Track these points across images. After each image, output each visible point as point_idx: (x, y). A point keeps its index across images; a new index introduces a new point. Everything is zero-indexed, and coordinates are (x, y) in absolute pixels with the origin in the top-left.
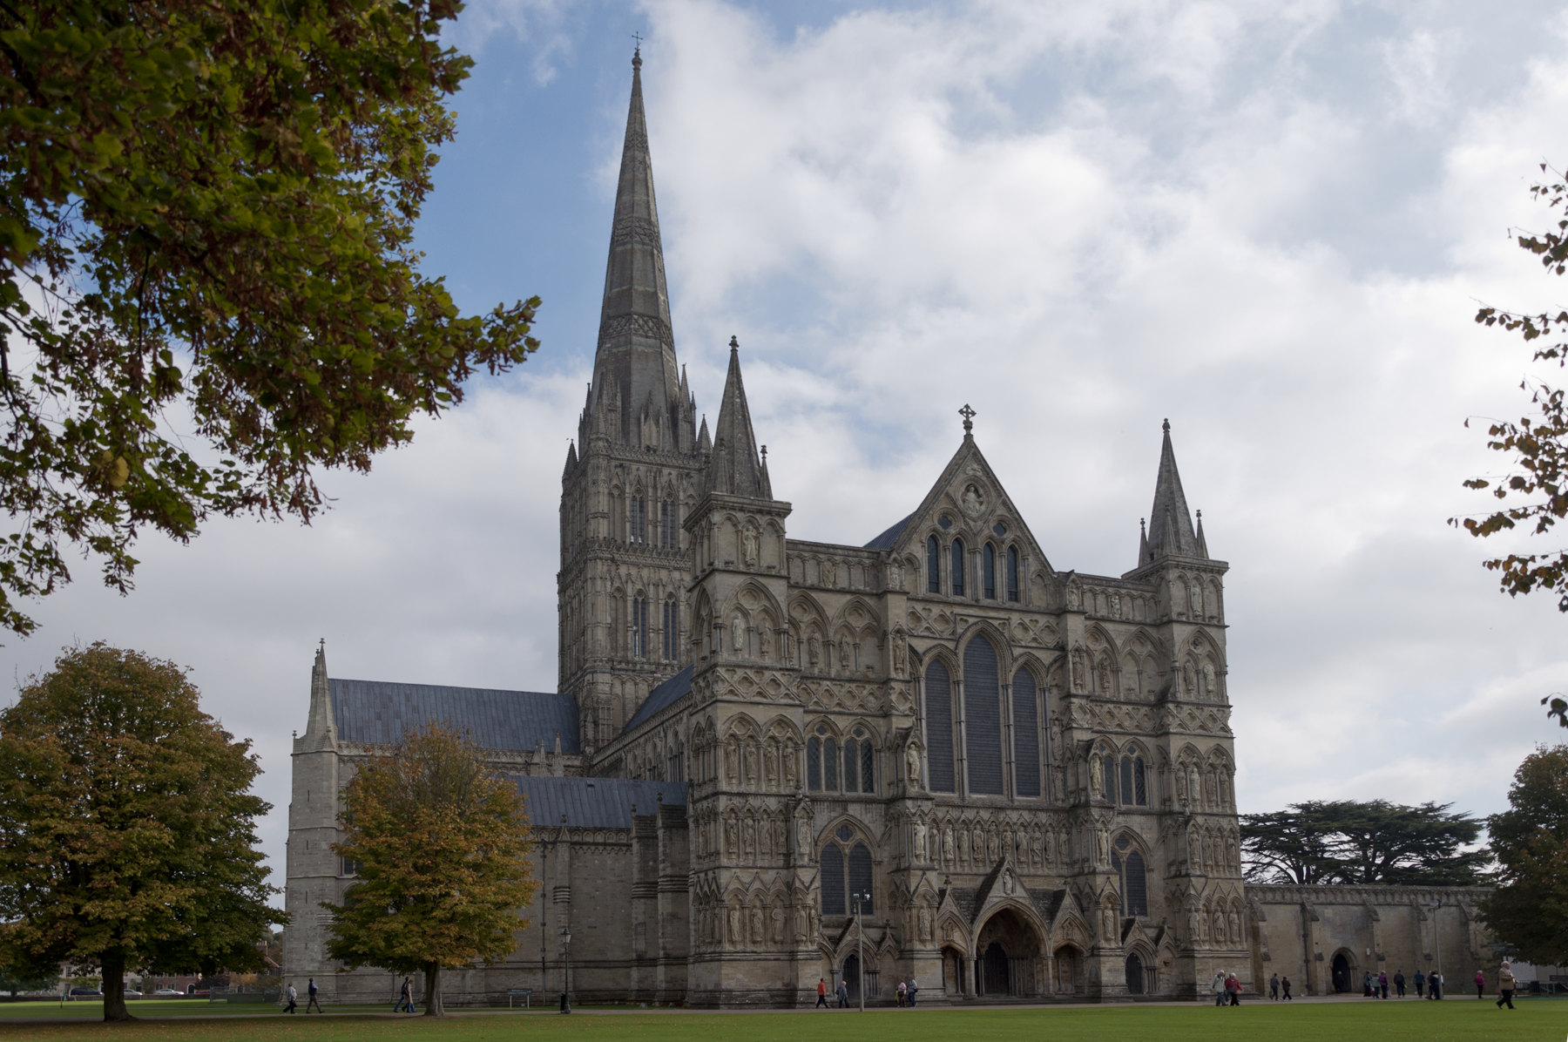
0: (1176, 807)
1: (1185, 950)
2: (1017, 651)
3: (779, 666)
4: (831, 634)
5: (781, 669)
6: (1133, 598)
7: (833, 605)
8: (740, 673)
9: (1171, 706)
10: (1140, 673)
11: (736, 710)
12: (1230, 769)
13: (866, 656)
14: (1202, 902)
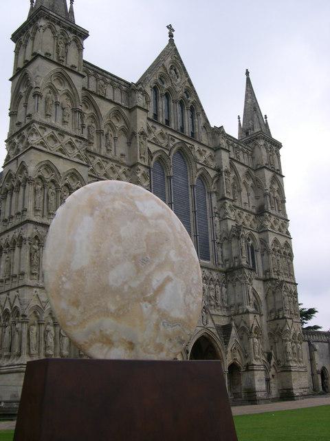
0: (273, 276)
1: (284, 366)
2: (199, 166)
3: (74, 133)
4: (102, 126)
5: (76, 136)
6: (244, 152)
7: (106, 109)
8: (49, 132)
9: (267, 214)
10: (248, 195)
11: (45, 158)
12: (291, 256)
13: (121, 147)
14: (292, 335)
